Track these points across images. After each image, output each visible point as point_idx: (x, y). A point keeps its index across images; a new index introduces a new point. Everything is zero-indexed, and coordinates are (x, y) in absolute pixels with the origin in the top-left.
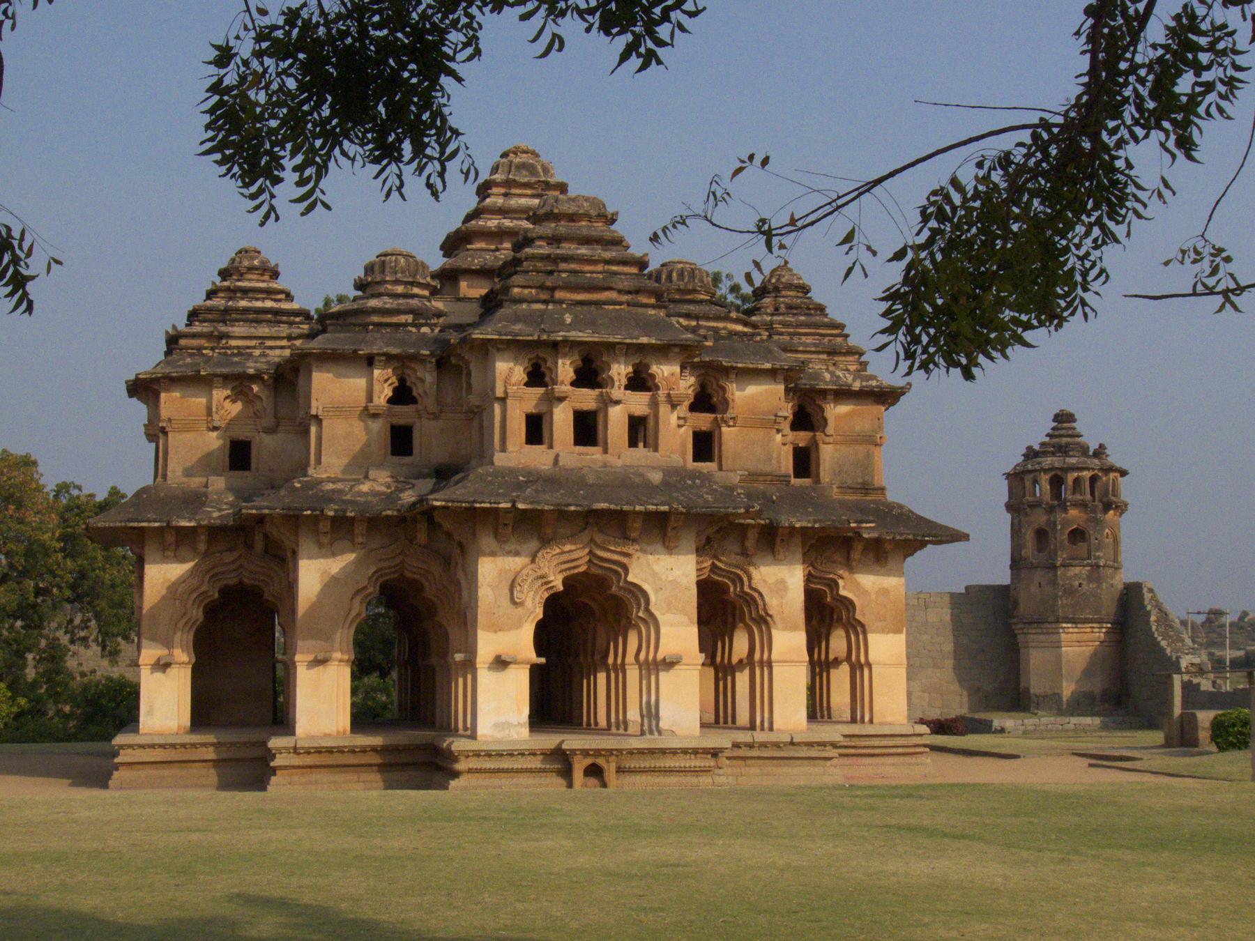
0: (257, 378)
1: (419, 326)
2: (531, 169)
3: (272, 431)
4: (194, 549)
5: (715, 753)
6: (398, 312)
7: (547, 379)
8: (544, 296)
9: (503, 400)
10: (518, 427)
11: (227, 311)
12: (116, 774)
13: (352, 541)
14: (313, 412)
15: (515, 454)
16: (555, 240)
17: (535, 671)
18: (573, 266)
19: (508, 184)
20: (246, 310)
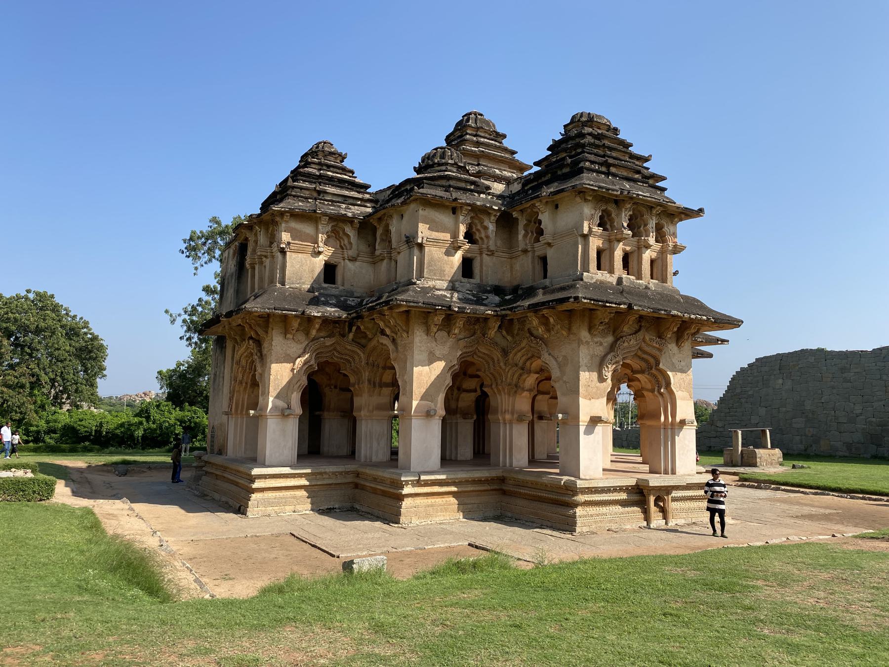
0: (350, 221)
1: (479, 193)
2: (488, 123)
3: (353, 259)
4: (307, 334)
6: (466, 181)
7: (608, 227)
8: (604, 169)
9: (585, 237)
10: (593, 255)
11: (320, 176)
12: (254, 496)
13: (449, 333)
14: (419, 241)
15: (594, 275)
18: (614, 154)
19: (478, 129)
20: (332, 177)
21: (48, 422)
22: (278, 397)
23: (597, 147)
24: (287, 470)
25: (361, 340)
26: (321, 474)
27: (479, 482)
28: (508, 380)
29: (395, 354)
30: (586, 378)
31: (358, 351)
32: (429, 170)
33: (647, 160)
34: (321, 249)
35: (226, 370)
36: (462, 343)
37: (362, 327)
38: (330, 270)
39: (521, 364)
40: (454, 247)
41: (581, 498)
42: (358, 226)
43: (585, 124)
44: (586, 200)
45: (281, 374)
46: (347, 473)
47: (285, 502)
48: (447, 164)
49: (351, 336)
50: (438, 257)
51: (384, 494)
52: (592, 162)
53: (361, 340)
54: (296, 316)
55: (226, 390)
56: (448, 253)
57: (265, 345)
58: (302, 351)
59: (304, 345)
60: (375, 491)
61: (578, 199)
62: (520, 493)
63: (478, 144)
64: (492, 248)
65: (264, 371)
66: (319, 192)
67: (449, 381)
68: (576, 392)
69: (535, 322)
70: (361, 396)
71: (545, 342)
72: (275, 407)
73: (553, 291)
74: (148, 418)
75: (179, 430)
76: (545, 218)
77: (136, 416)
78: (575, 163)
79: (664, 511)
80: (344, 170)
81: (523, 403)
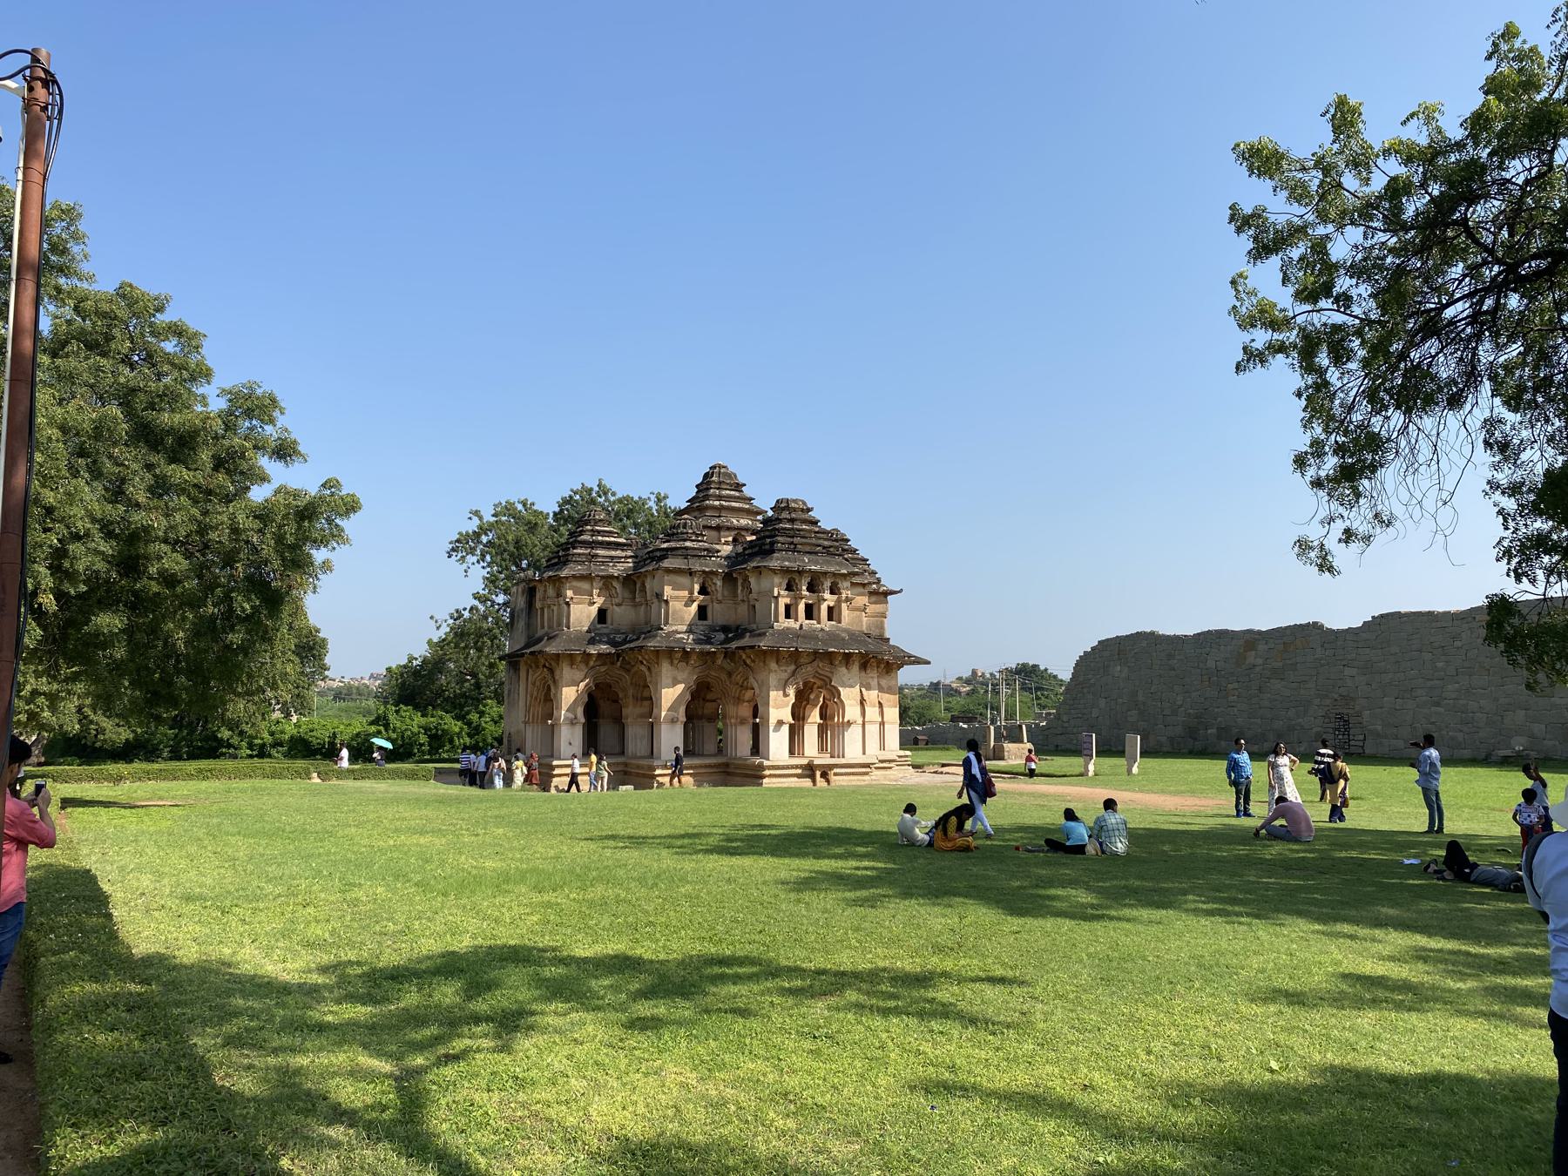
2: (729, 475)
3: (619, 605)
5: (867, 766)
10: (782, 610)
15: (783, 623)
16: (792, 521)
17: (792, 727)
21: (272, 734)
25: (627, 667)
27: (710, 766)
30: (775, 695)
38: (602, 614)
40: (691, 600)
41: (767, 772)
43: (783, 509)
45: (569, 695)
50: (680, 609)
51: (644, 776)
53: (627, 667)
55: (522, 703)
56: (686, 605)
57: (557, 673)
60: (638, 775)
63: (720, 498)
67: (688, 697)
74: (387, 726)
75: (423, 739)
76: (752, 580)
77: (372, 723)
78: (772, 544)
81: (745, 710)
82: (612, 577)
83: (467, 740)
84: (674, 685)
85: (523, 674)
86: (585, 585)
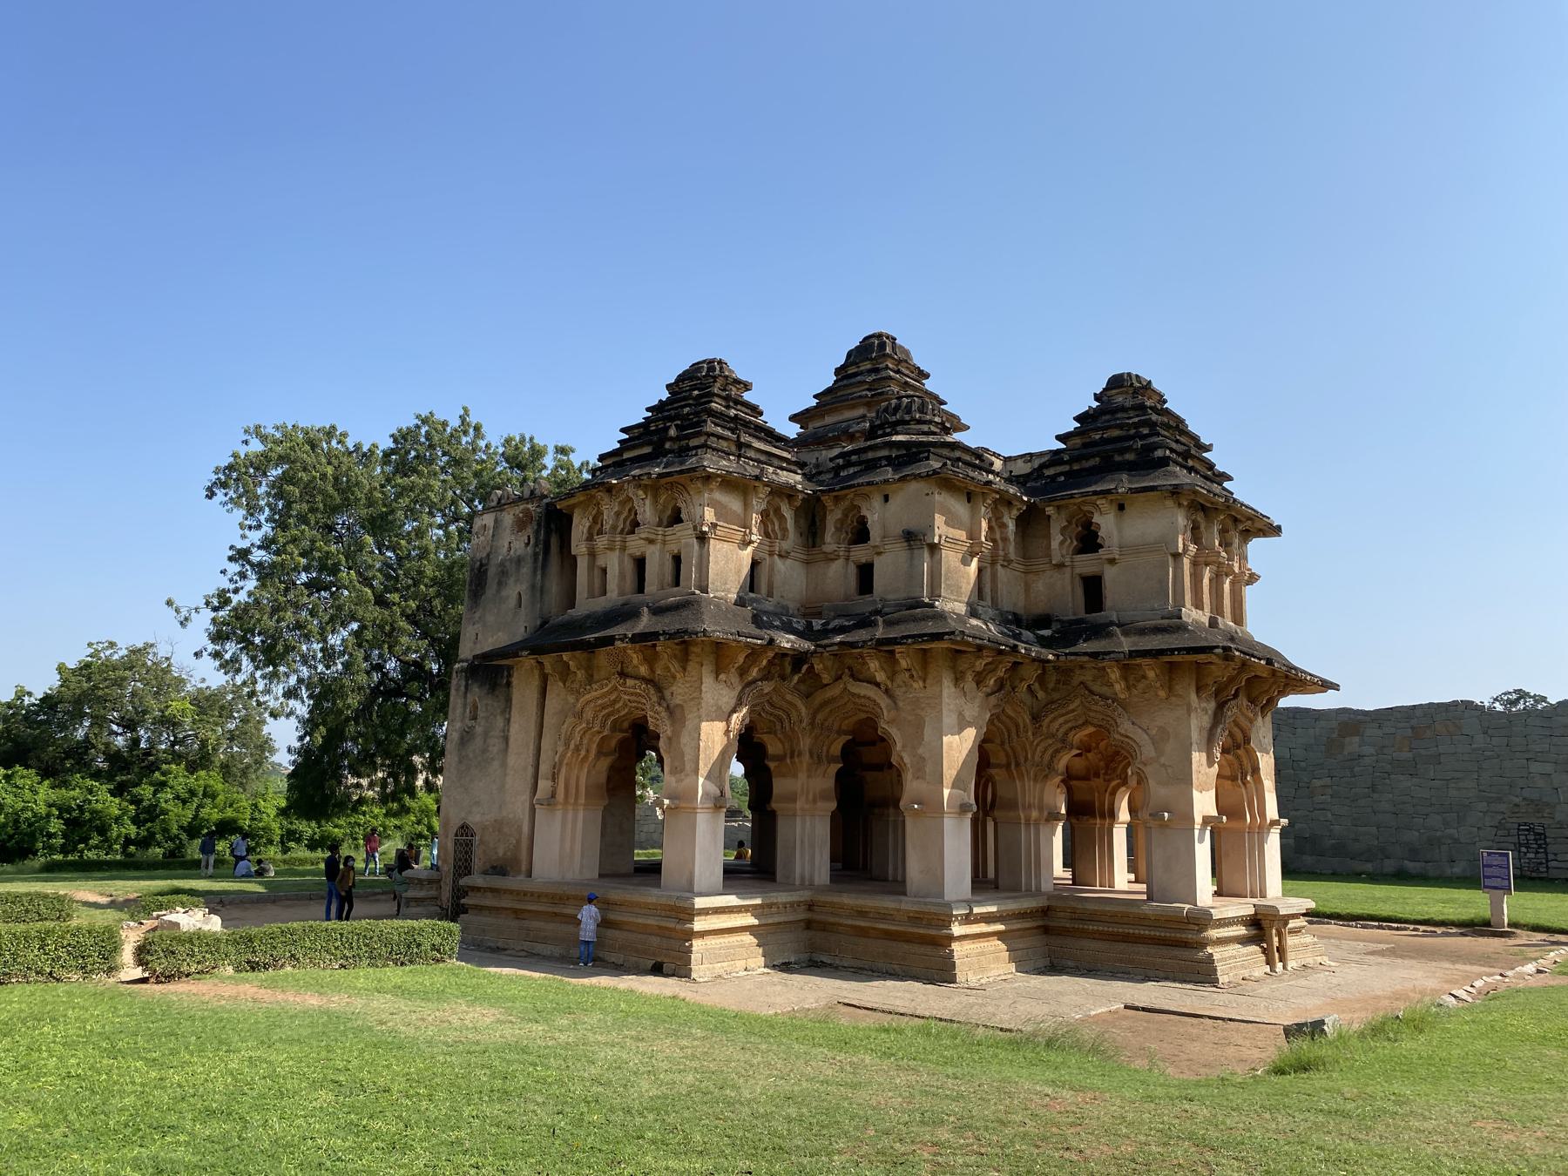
2: (907, 353)
9: (1177, 556)
12: (697, 945)
19: (900, 361)
22: (708, 778)
23: (1167, 427)
24: (732, 900)
25: (813, 684)
26: (770, 906)
28: (1037, 758)
29: (893, 713)
30: (1198, 758)
31: (799, 704)
32: (899, 428)
33: (1208, 448)
34: (754, 538)
35: (514, 728)
36: (993, 700)
37: (818, 667)
39: (1060, 734)
41: (1214, 933)
42: (798, 503)
44: (1180, 505)
46: (799, 904)
47: (729, 957)
48: (930, 422)
49: (796, 678)
52: (1172, 450)
54: (747, 645)
56: (965, 562)
57: (678, 692)
58: (733, 702)
59: (736, 693)
60: (862, 932)
61: (1170, 503)
62: (1083, 931)
64: (1012, 556)
65: (676, 735)
66: (740, 445)
68: (1184, 779)
69: (1114, 674)
70: (795, 776)
71: (1124, 705)
72: (706, 794)
73: (1142, 632)
75: (55, 826)
76: (1106, 522)
79: (1281, 950)
80: (756, 411)
82: (787, 492)
83: (132, 830)
84: (960, 730)
85: (524, 690)
86: (734, 503)
